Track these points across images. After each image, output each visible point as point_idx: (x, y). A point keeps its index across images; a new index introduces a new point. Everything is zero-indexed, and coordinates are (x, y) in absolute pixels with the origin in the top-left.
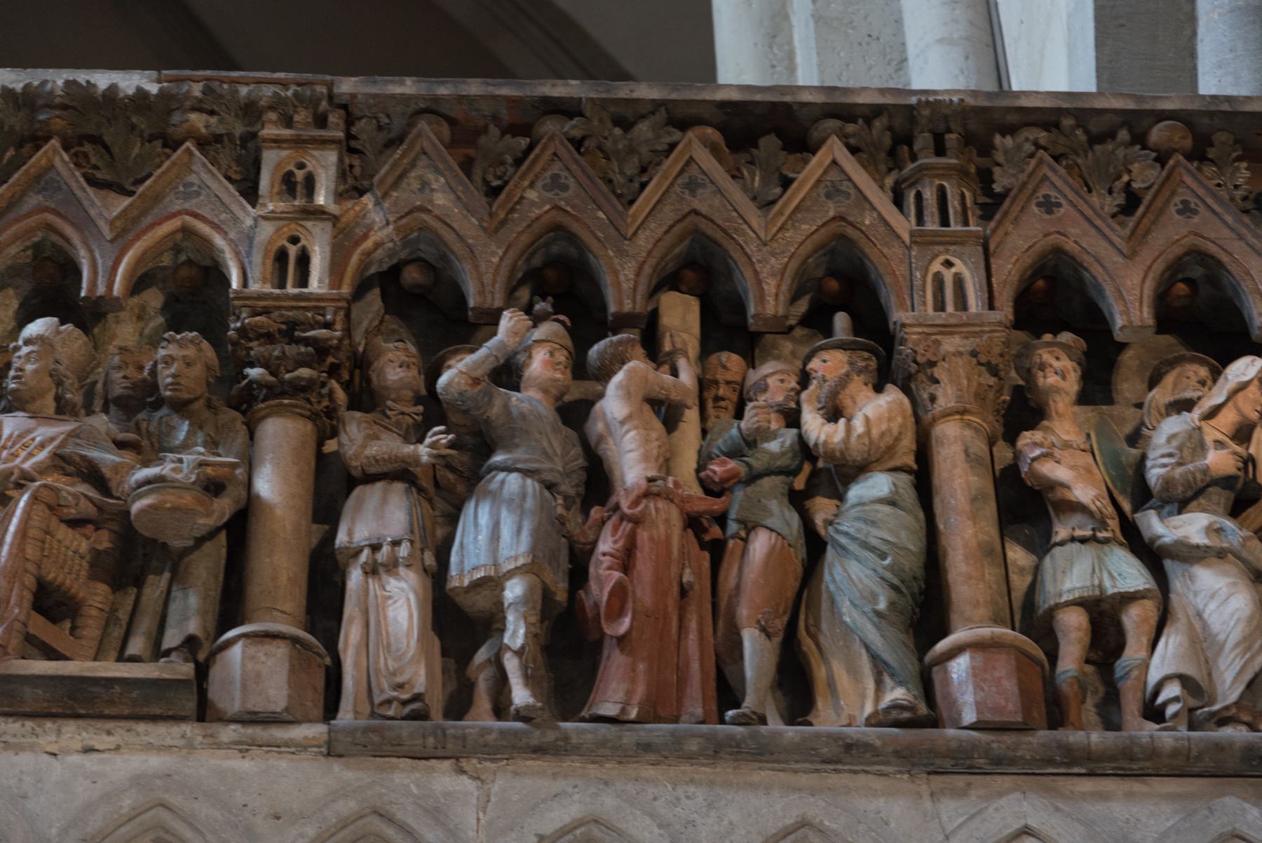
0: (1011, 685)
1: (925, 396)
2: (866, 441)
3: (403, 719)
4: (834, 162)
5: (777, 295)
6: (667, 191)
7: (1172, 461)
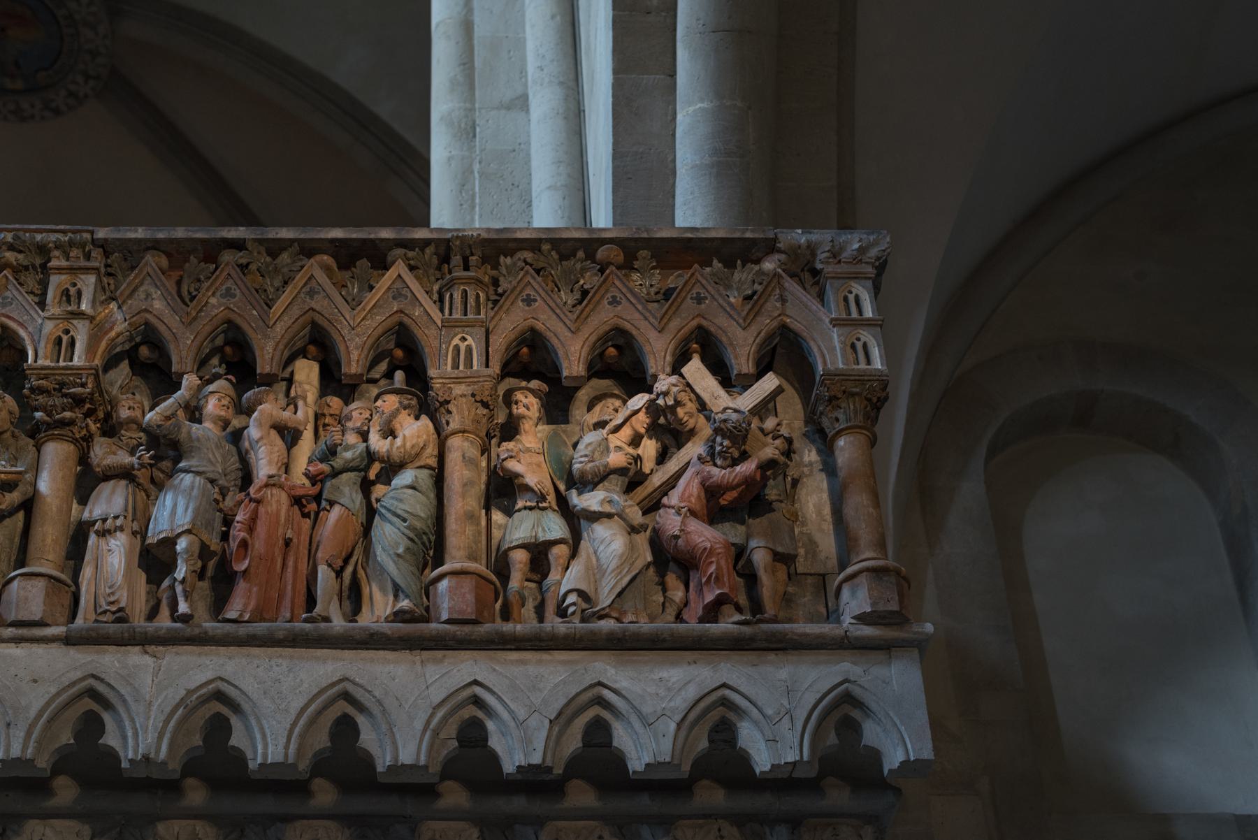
0: (470, 597)
1: (444, 422)
2: (402, 450)
4: (399, 276)
5: (358, 361)
6: (296, 296)
7: (586, 459)
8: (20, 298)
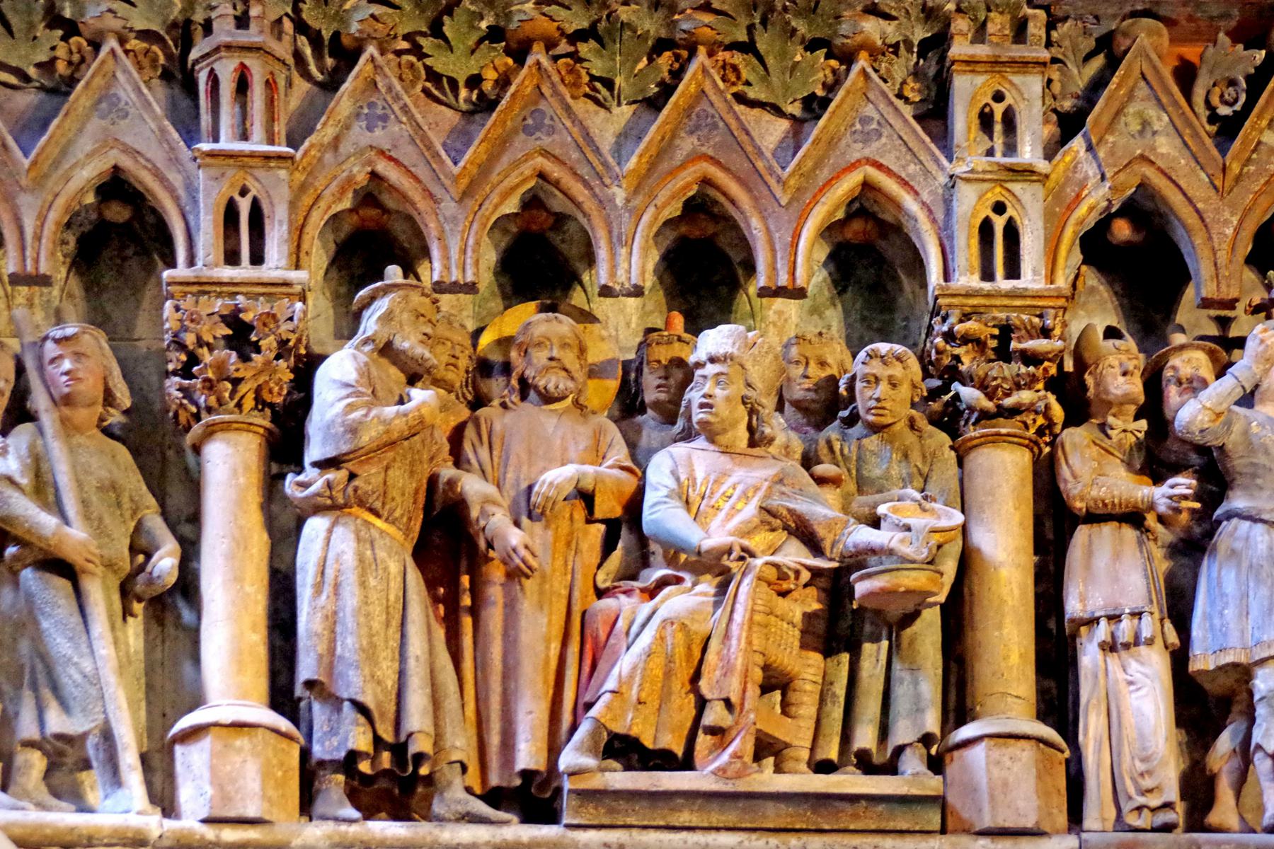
3: (1154, 830)
8: (898, 124)
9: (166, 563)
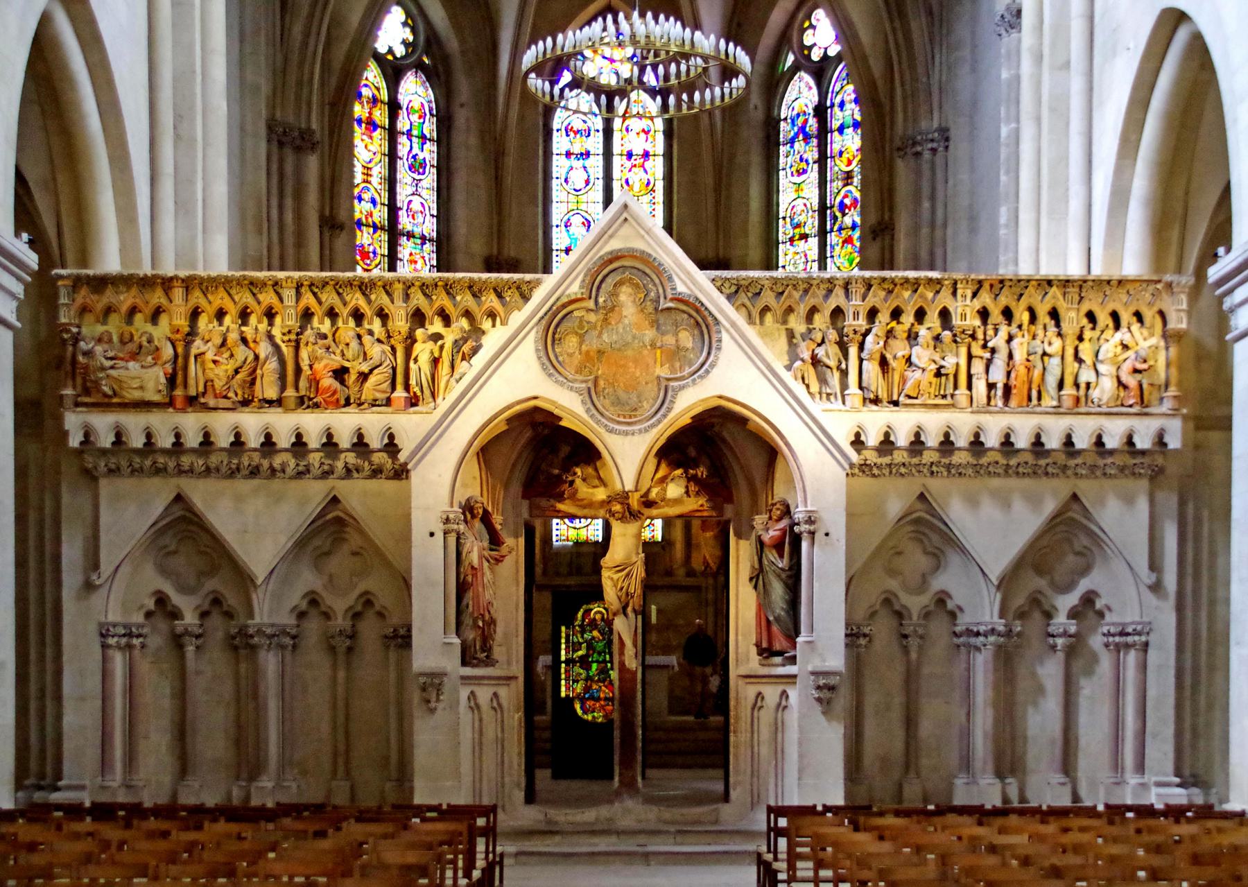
9: (843, 366)
